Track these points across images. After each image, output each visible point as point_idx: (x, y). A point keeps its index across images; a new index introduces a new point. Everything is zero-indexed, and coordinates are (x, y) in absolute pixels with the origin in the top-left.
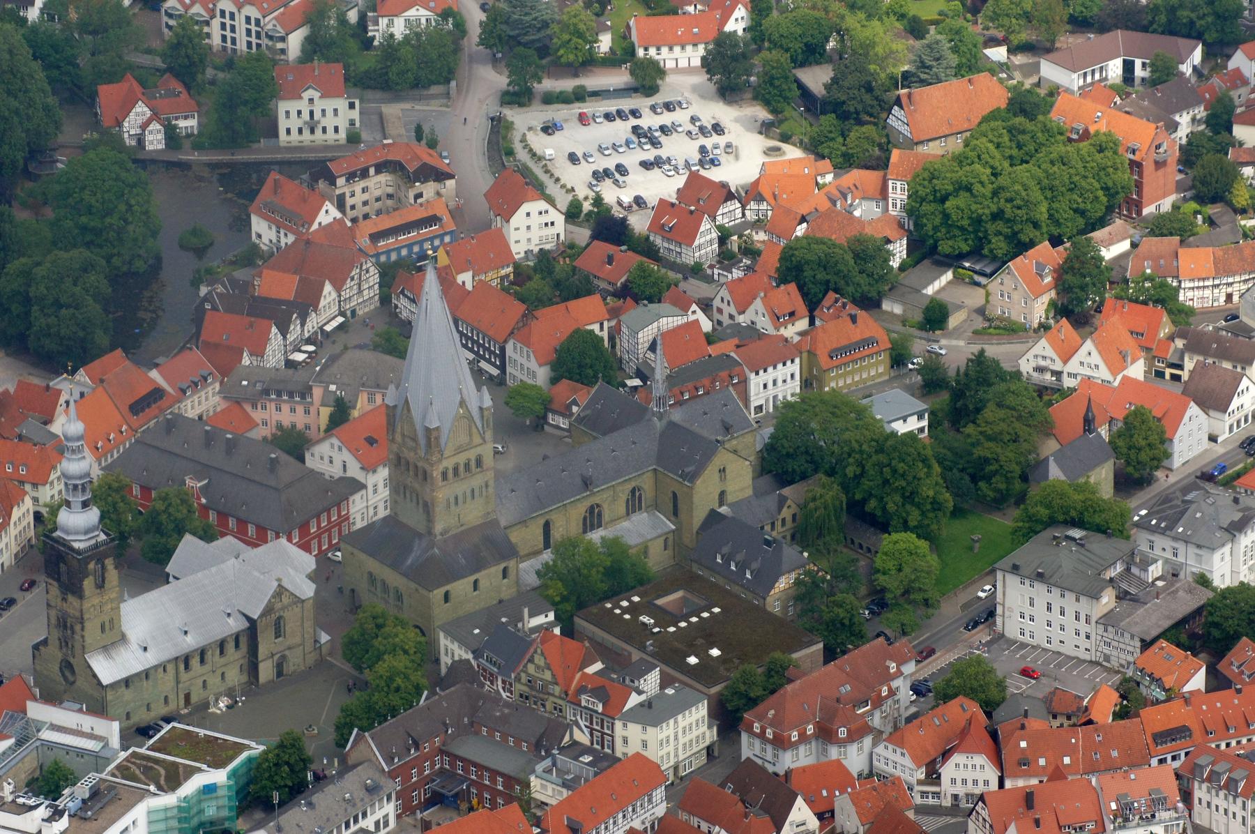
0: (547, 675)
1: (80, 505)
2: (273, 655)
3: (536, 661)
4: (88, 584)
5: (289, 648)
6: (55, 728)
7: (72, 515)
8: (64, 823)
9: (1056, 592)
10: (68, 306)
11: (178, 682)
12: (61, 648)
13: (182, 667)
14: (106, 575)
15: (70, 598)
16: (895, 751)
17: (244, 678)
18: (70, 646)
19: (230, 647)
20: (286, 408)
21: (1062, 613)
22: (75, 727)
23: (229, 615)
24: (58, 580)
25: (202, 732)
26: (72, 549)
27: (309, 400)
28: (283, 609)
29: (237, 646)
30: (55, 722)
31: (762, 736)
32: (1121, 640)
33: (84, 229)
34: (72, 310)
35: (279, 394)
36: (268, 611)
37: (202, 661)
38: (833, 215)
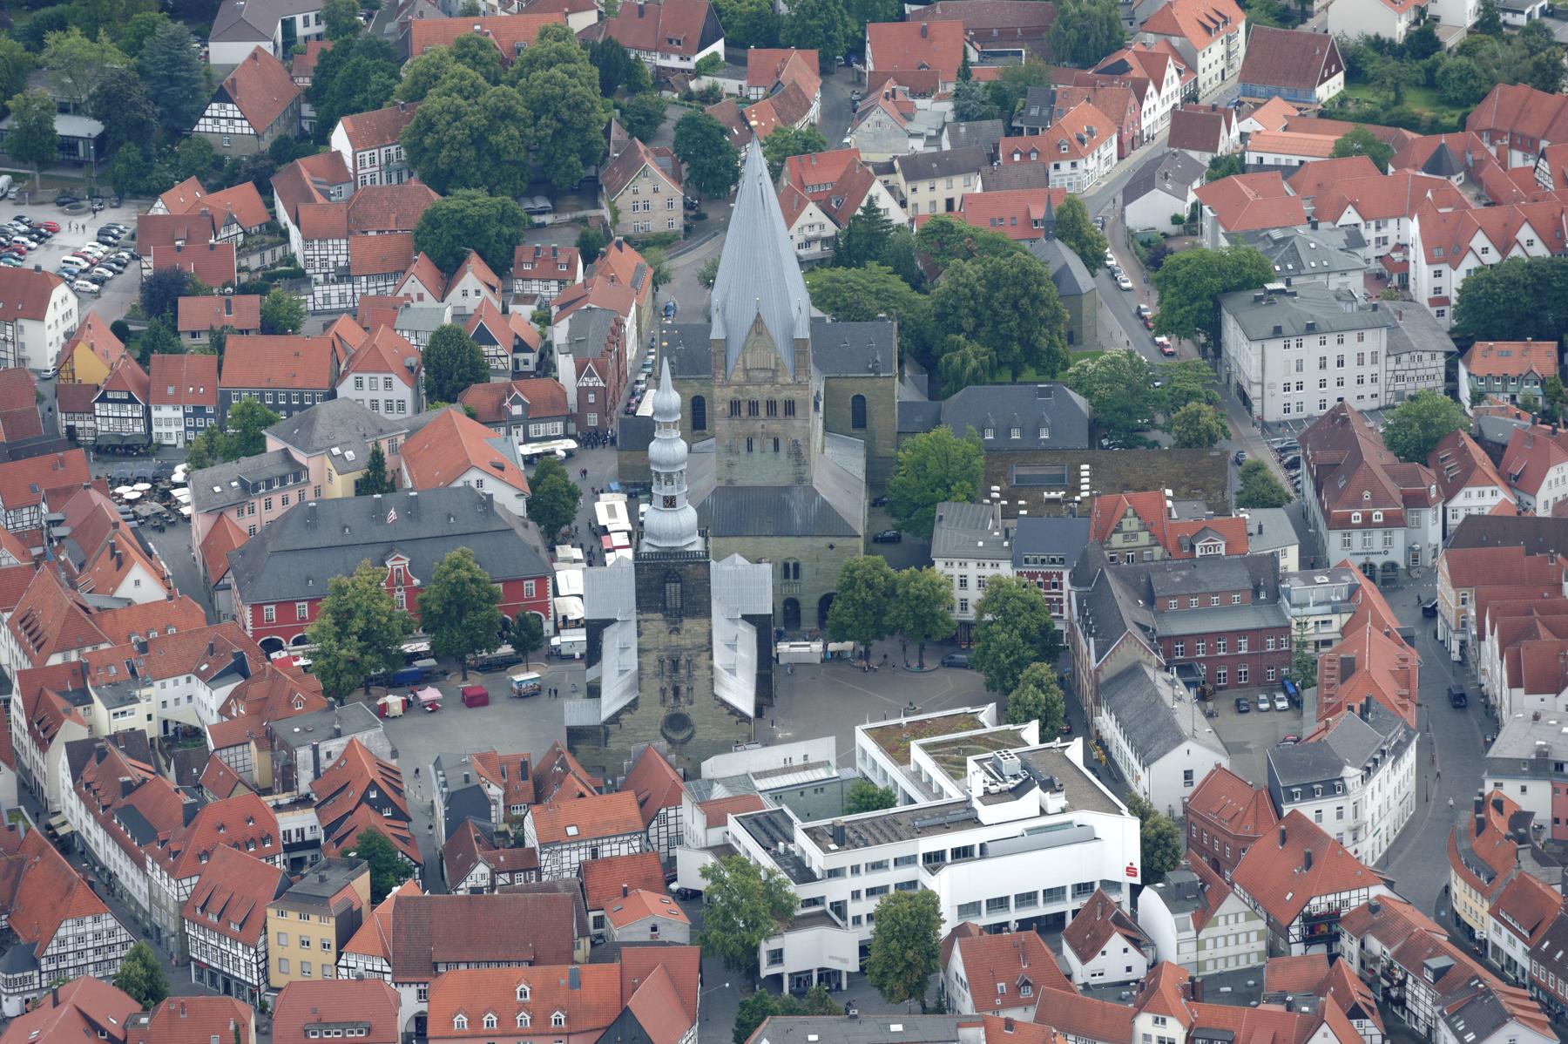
0: (1144, 538)
3: (1126, 527)
7: (679, 514)
9: (1332, 339)
12: (664, 701)
15: (687, 623)
16: (1481, 494)
18: (683, 689)
20: (277, 500)
21: (1340, 363)
22: (783, 765)
24: (664, 609)
25: (904, 721)
27: (303, 480)
31: (1367, 522)
32: (1420, 365)
35: (269, 484)
38: (375, 194)
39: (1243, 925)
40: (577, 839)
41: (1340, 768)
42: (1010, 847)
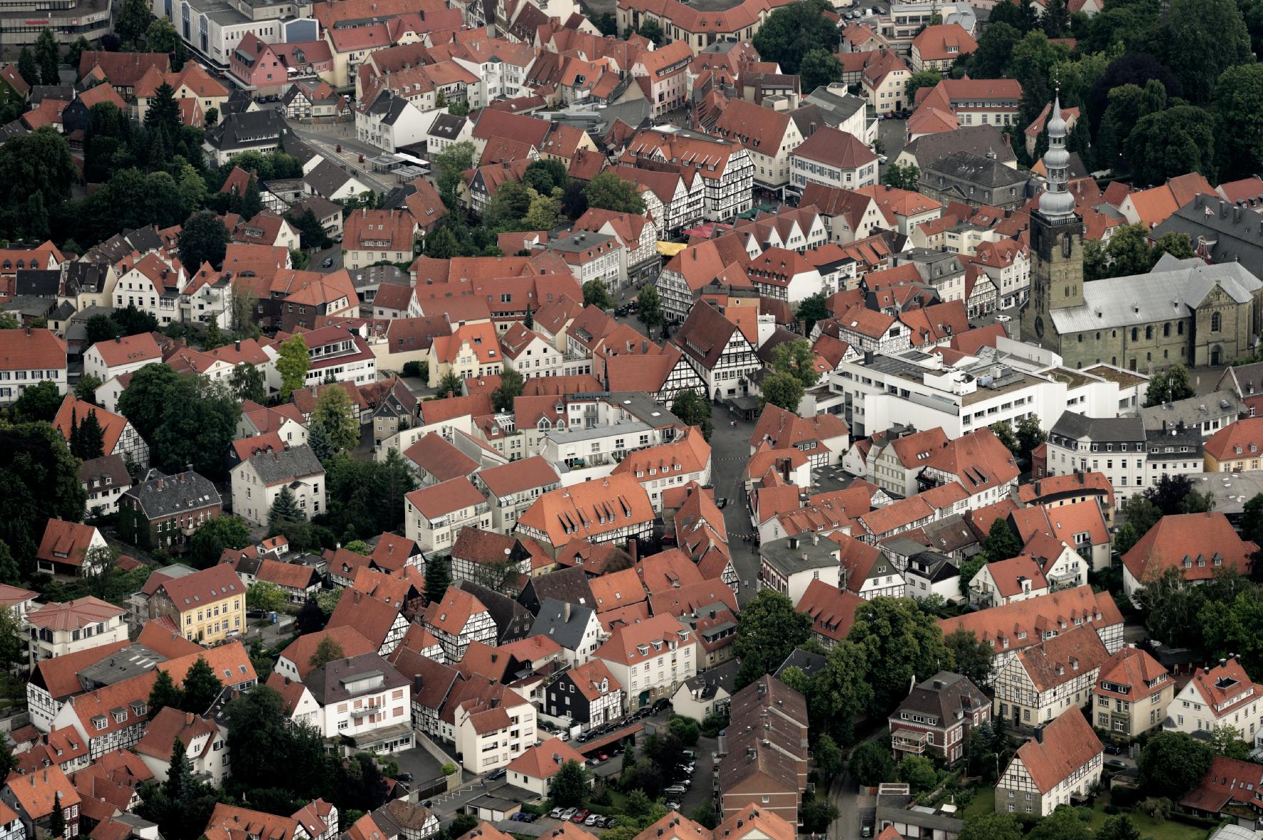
1: (1056, 187)
2: (1208, 343)
4: (1056, 252)
5: (1223, 341)
6: (1012, 357)
8: (972, 387)
10: (1172, 144)
11: (1125, 348)
13: (1129, 336)
14: (1073, 248)
17: (1185, 360)
19: (1174, 330)
23: (1176, 305)
26: (1049, 223)
28: (1220, 306)
29: (1180, 332)
30: (1015, 353)
33: (1231, 122)
34: (1175, 148)
36: (1206, 305)
37: (1148, 336)
39: (895, 466)
40: (852, 329)
41: (1082, 435)
42: (922, 401)
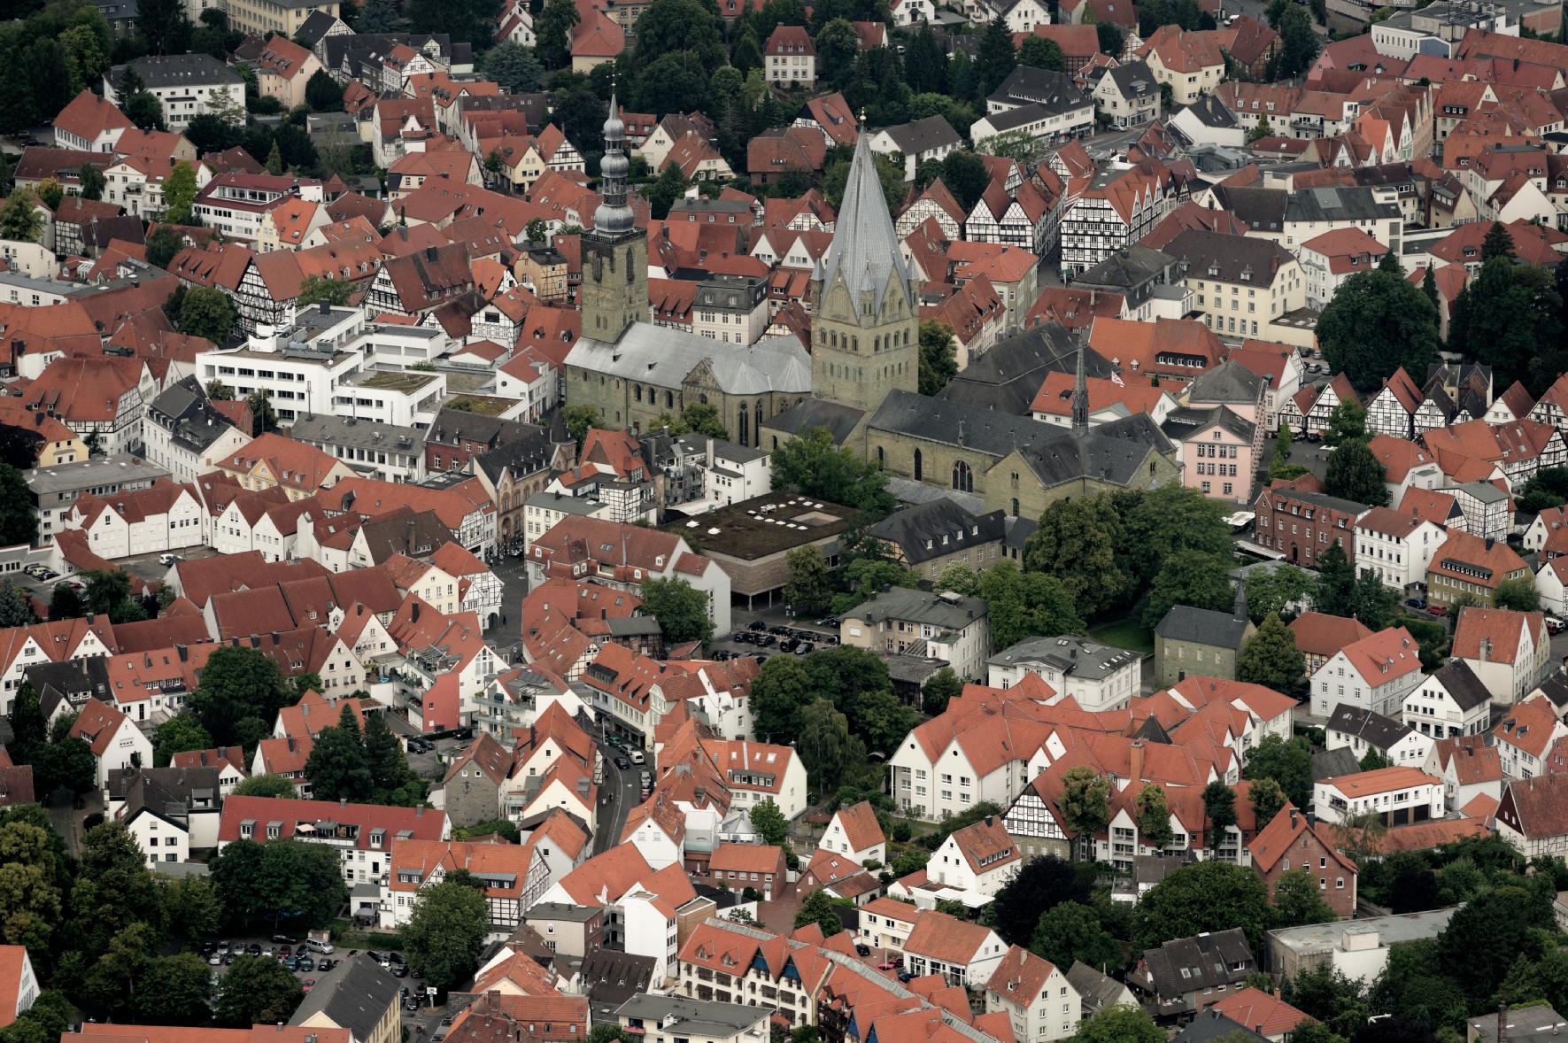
11: (627, 406)
13: (632, 393)
28: (707, 388)
